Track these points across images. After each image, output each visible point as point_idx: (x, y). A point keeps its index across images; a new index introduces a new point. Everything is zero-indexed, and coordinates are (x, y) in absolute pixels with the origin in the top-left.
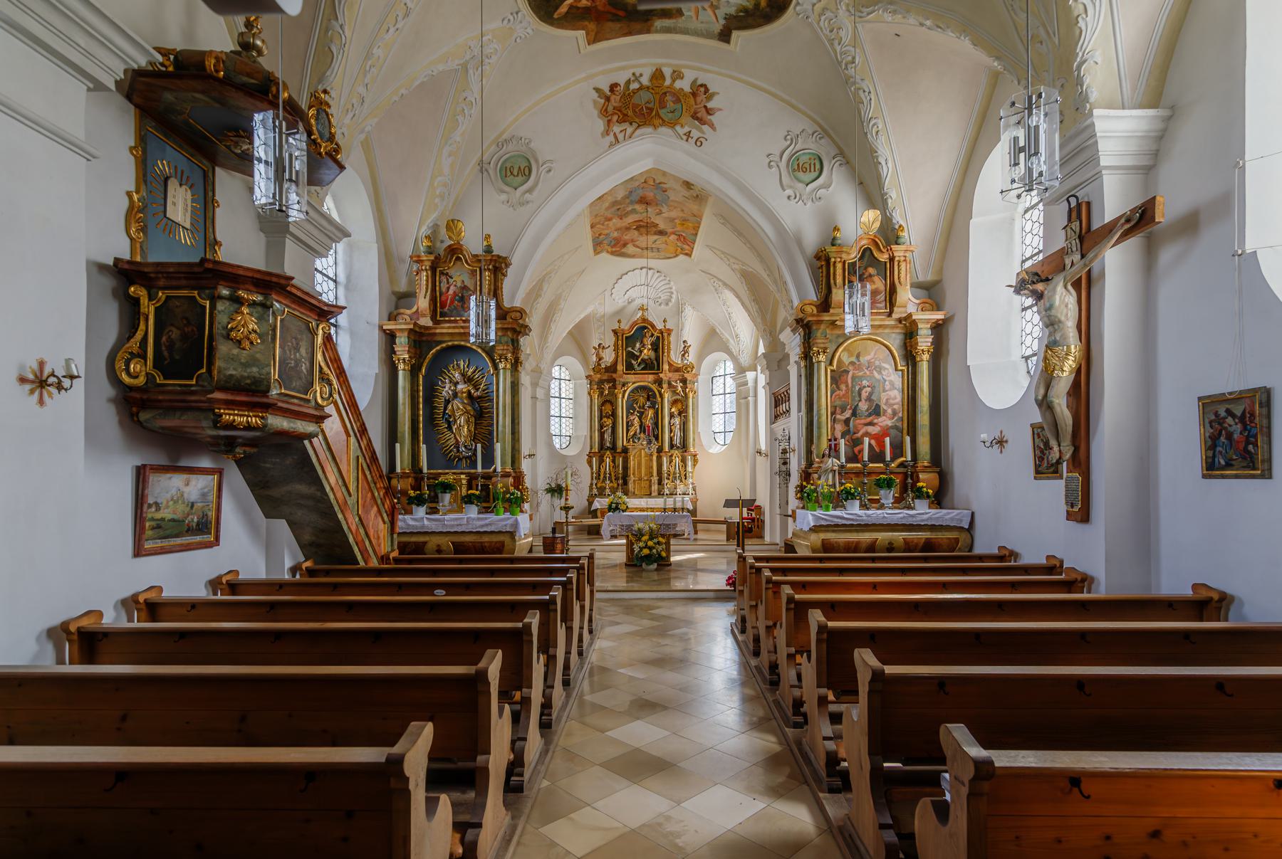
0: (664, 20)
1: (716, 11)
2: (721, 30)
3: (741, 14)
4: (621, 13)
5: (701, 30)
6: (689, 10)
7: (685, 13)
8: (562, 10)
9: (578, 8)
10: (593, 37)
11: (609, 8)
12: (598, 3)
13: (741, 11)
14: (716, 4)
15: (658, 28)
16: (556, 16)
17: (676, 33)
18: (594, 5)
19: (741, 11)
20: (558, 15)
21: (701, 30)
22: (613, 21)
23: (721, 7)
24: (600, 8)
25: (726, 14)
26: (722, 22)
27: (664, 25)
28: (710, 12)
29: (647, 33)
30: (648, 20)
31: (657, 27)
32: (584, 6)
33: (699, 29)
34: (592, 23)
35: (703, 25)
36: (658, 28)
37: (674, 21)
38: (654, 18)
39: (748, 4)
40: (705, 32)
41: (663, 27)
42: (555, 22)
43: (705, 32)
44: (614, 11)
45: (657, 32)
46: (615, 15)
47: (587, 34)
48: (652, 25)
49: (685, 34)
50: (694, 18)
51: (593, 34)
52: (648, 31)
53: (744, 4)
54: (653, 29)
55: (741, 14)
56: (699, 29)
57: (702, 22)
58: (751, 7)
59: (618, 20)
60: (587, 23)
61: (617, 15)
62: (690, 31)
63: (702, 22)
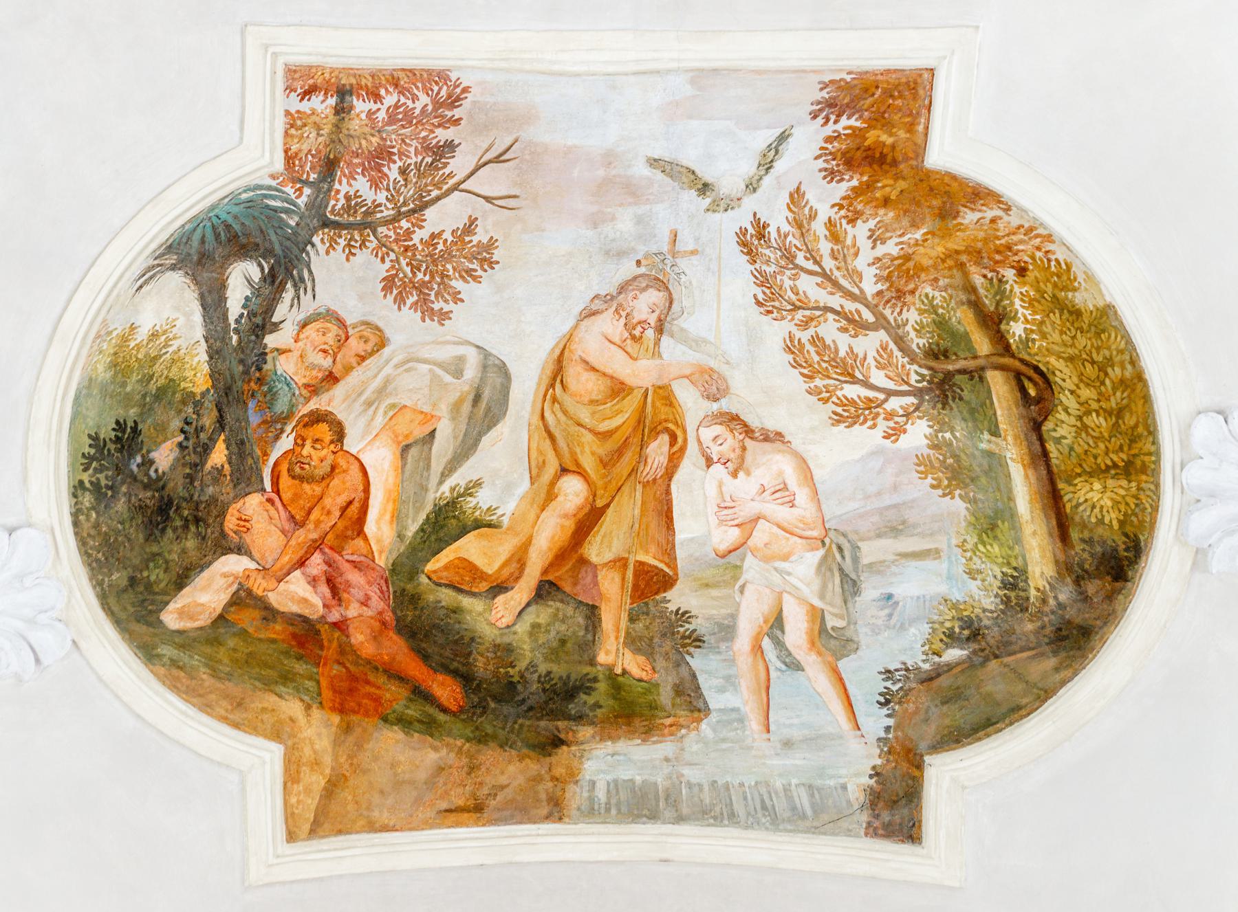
0: (622, 745)
1: (843, 665)
2: (876, 773)
3: (954, 654)
4: (446, 690)
5: (787, 789)
6: (730, 682)
7: (715, 700)
8: (204, 598)
9: (269, 613)
10: (312, 803)
11: (396, 648)
12: (353, 611)
13: (951, 638)
14: (840, 623)
15: (601, 794)
16: (171, 618)
17: (680, 819)
18: (334, 616)
19: (951, 638)
20: (182, 613)
21: (787, 789)
22: (404, 723)
23: (863, 634)
24: (358, 638)
25: (888, 674)
26: (876, 722)
27: (625, 774)
28: (816, 675)
29: (548, 818)
30: (558, 742)
31: (593, 784)
32: (295, 608)
33: (778, 784)
34: (316, 713)
35: (796, 760)
36: (601, 794)
37: (660, 749)
38: (585, 732)
39: (973, 586)
40: (803, 800)
41: (616, 781)
42: (166, 651)
43: (803, 800)
44: (415, 669)
45: (591, 813)
46: (420, 694)
47: (292, 775)
48: (572, 776)
49: (718, 820)
50: (754, 725)
51: (317, 781)
52: (556, 810)
53: (957, 596)
54: (576, 796)
55: (954, 654)
56: (778, 784)
57: (788, 744)
58: (989, 602)
59: (429, 727)
60: (292, 707)
61: (428, 698)
62: (739, 808)
63: (788, 744)
